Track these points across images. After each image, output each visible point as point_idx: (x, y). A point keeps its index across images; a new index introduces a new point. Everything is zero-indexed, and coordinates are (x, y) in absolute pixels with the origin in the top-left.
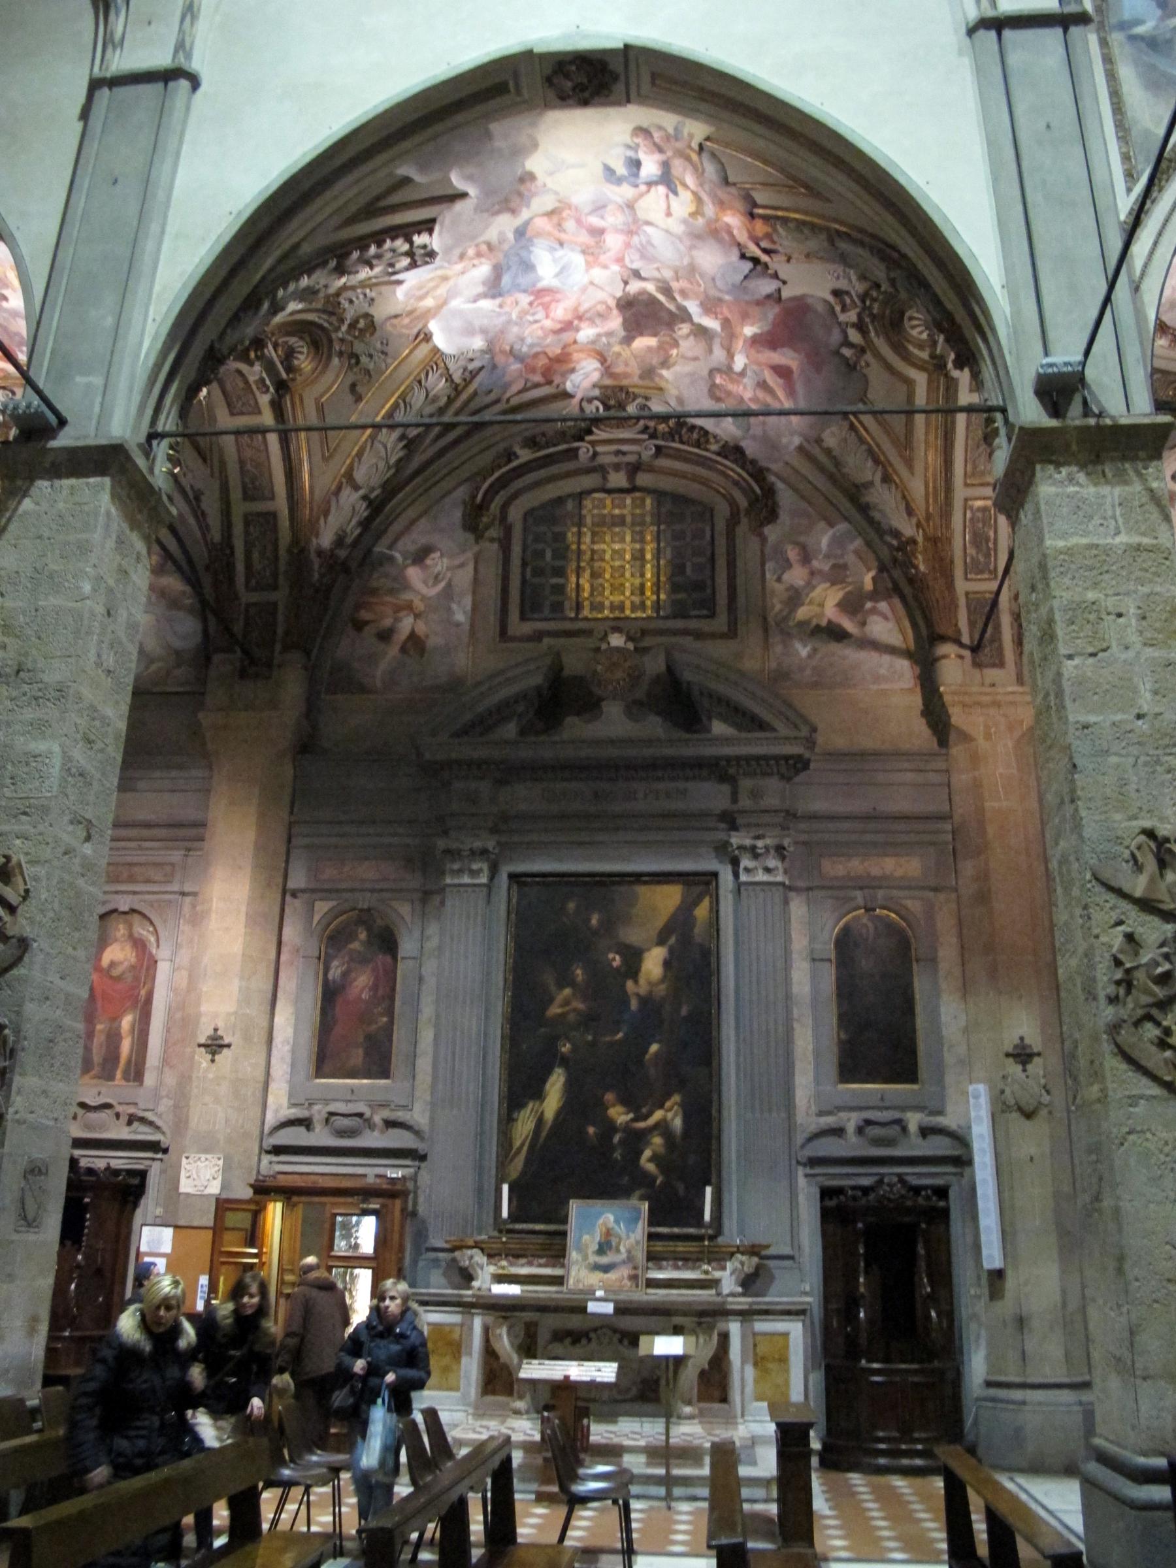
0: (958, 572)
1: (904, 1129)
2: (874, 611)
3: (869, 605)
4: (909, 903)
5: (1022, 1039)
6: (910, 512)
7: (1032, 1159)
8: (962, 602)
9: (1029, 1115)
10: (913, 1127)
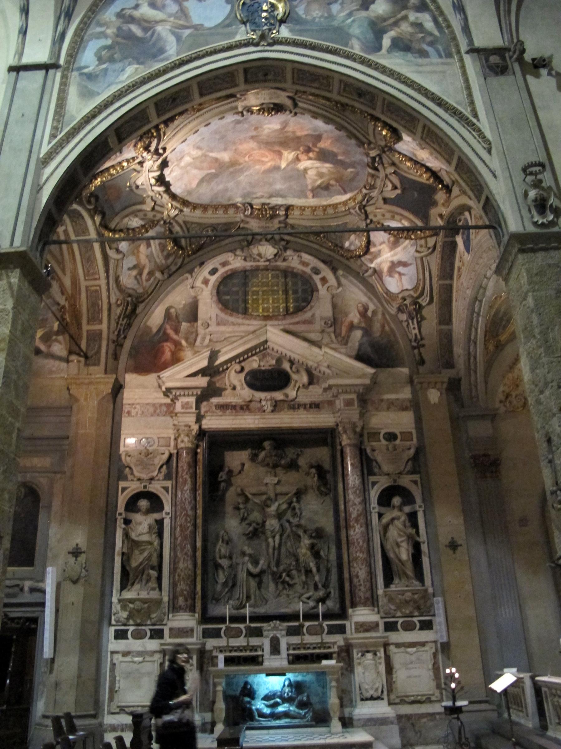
0: (84, 321)
1: (22, 589)
2: (56, 341)
3: (54, 337)
4: (41, 480)
5: (77, 545)
6: (63, 293)
7: (73, 604)
8: (85, 335)
9: (75, 582)
10: (26, 589)
